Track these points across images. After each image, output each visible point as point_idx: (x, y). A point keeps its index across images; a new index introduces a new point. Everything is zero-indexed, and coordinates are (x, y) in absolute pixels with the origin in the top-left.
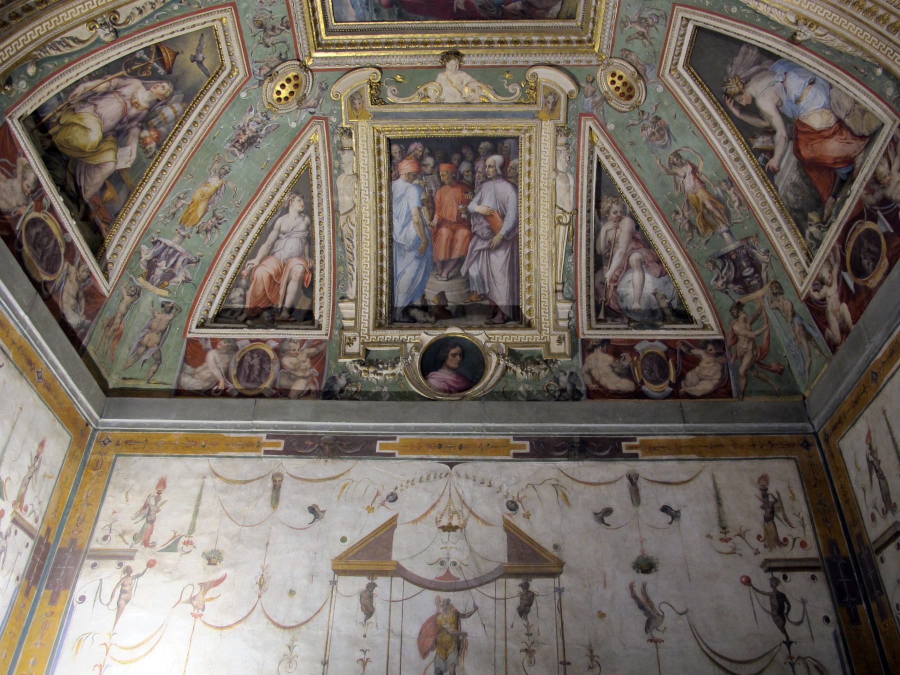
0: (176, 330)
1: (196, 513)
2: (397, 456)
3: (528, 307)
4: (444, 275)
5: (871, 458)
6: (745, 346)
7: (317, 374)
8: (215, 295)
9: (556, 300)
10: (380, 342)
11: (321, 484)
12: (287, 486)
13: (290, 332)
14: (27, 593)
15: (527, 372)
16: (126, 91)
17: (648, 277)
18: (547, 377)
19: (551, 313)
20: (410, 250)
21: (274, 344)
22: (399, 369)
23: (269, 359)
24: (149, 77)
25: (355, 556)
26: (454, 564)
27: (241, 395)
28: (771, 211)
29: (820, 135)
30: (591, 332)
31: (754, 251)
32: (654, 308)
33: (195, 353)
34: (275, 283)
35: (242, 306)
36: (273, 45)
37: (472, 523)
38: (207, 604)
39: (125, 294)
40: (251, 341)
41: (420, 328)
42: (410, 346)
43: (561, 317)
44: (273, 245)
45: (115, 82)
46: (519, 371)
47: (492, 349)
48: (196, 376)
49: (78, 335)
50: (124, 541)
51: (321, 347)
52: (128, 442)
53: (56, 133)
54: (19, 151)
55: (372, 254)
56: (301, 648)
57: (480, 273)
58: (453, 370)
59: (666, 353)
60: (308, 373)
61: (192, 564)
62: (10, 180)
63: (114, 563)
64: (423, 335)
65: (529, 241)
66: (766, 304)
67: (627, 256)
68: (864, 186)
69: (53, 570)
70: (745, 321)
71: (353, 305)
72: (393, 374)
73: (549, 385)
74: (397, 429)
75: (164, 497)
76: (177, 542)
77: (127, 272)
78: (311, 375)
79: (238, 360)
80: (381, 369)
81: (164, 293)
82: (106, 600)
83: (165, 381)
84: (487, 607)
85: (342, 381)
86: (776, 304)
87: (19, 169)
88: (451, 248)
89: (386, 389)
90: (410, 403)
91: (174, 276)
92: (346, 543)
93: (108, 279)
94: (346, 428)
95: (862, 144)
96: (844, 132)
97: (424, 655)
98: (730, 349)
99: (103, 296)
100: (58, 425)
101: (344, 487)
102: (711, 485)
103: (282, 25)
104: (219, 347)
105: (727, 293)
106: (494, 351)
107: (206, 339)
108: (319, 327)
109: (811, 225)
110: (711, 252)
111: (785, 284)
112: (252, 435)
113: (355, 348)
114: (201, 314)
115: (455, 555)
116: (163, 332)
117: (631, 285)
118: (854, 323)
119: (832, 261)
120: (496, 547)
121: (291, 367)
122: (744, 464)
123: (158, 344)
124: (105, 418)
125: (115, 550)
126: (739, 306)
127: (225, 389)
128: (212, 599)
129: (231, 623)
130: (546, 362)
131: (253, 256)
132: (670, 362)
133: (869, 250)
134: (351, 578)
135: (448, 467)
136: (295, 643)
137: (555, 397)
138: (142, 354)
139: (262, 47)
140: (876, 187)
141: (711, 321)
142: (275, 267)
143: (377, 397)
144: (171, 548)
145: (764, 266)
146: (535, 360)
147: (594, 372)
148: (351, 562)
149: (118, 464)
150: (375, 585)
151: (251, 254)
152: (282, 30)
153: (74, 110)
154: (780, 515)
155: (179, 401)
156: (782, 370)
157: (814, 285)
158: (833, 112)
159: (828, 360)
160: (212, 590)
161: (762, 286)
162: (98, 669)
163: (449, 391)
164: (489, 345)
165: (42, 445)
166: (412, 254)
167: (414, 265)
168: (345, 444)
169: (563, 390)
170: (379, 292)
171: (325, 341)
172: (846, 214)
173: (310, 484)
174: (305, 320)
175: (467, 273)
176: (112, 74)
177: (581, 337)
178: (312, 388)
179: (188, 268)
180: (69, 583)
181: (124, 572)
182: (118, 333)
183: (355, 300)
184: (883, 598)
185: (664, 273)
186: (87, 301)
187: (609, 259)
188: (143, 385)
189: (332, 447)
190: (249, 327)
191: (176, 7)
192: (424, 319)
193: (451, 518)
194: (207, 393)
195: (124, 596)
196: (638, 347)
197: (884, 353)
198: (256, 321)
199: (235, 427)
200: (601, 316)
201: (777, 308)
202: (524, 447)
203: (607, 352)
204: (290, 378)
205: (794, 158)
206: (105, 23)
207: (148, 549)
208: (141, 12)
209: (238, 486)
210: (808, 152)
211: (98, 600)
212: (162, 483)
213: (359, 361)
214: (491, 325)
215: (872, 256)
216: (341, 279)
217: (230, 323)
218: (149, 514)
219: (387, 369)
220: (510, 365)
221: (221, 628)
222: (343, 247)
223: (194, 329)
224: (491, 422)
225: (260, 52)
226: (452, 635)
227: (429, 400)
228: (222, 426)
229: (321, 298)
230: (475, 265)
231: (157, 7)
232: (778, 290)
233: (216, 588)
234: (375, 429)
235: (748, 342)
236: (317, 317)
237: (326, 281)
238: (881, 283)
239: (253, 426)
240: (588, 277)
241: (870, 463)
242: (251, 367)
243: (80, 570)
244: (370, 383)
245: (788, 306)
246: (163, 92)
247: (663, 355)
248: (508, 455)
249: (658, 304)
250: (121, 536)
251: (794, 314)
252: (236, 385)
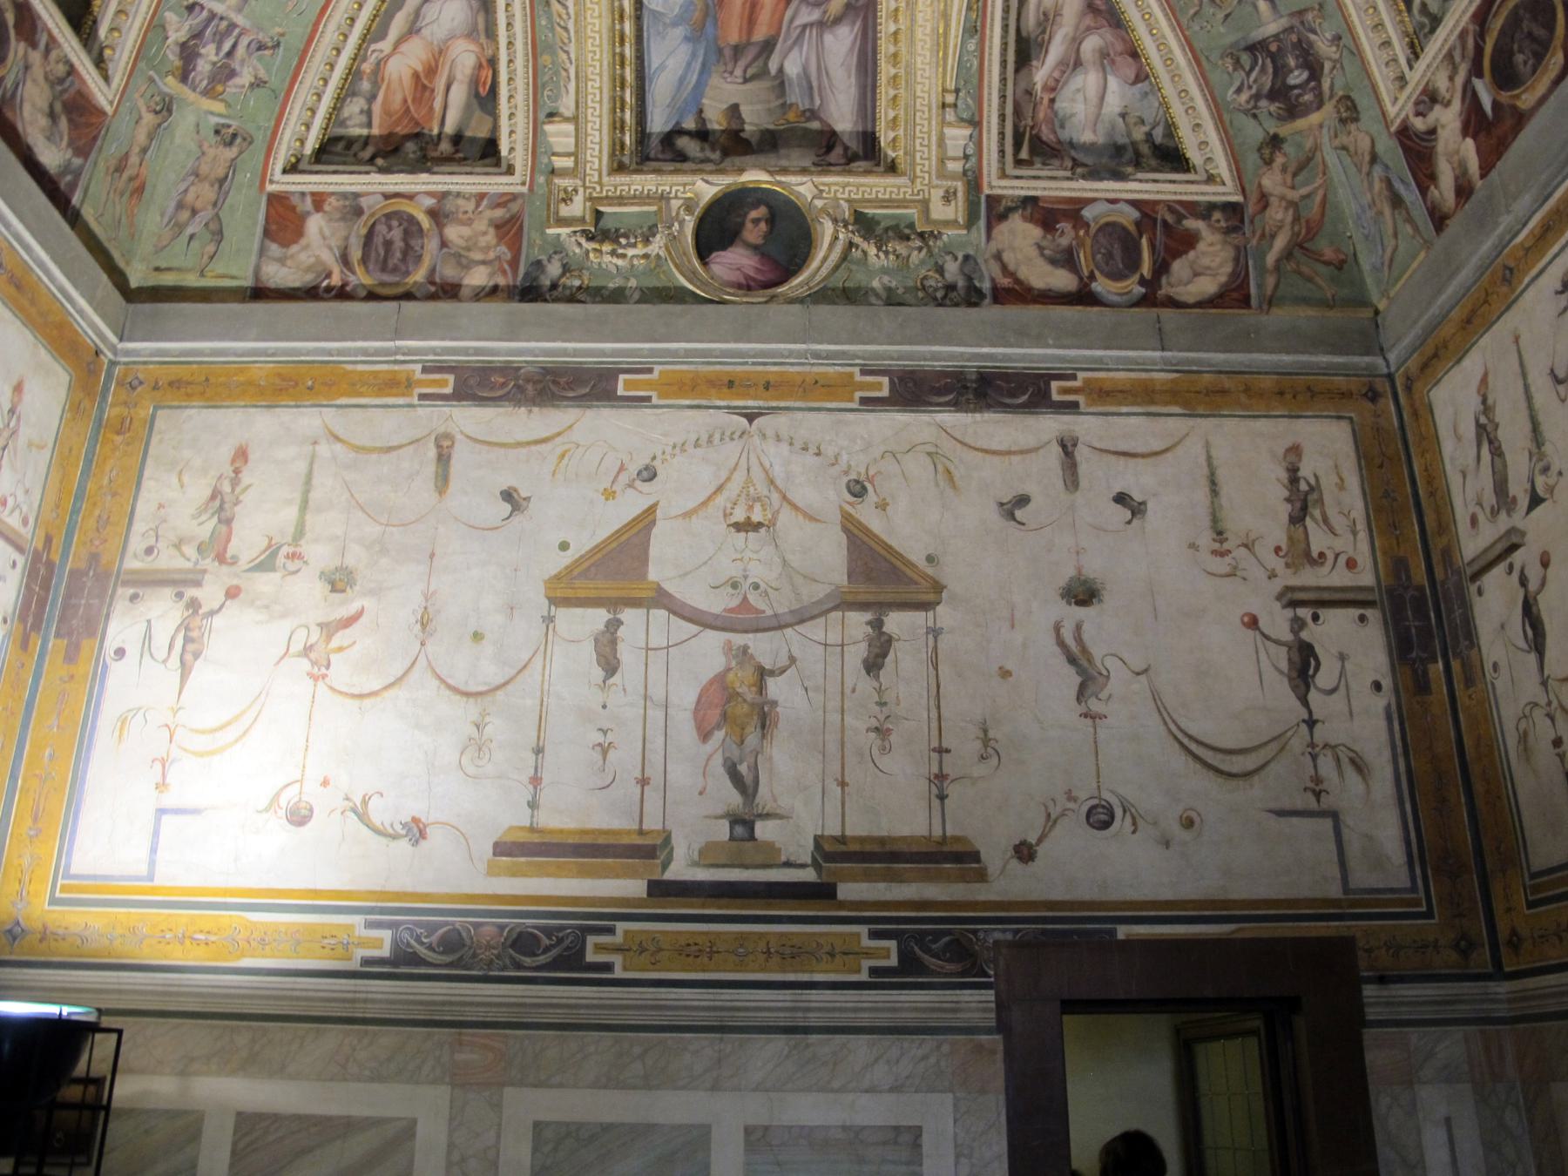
0: (245, 177)
1: (304, 505)
2: (655, 401)
3: (891, 135)
4: (738, 72)
5: (1483, 420)
6: (1279, 216)
7: (509, 256)
8: (313, 111)
9: (944, 123)
10: (621, 197)
11: (524, 451)
12: (462, 456)
13: (455, 179)
14: (25, 644)
15: (887, 253)
17: (1113, 83)
18: (923, 262)
19: (935, 148)
20: (675, 24)
21: (429, 202)
22: (657, 246)
23: (421, 230)
25: (584, 574)
26: (756, 587)
27: (372, 296)
30: (1004, 183)
31: (1312, 37)
32: (1122, 140)
33: (283, 221)
34: (425, 87)
35: (365, 132)
37: (786, 517)
38: (333, 657)
39: (143, 109)
40: (387, 196)
41: (694, 172)
42: (675, 204)
43: (950, 153)
44: (417, 14)
46: (872, 251)
47: (824, 210)
48: (289, 262)
49: (62, 186)
50: (183, 555)
51: (515, 207)
52: (176, 384)
55: (604, 31)
56: (496, 728)
57: (805, 69)
58: (755, 248)
59: (1138, 224)
60: (492, 255)
61: (306, 591)
63: (168, 592)
64: (700, 185)
65: (897, 10)
66: (1325, 139)
67: (1076, 42)
69: (65, 607)
70: (1284, 169)
71: (570, 127)
72: (646, 256)
73: (925, 278)
74: (653, 353)
75: (246, 478)
76: (274, 555)
77: (142, 65)
78: (498, 258)
79: (364, 231)
80: (624, 247)
81: (218, 107)
82: (161, 653)
83: (234, 272)
84: (810, 658)
85: (554, 269)
86: (1344, 139)
88: (751, 21)
89: (633, 283)
90: (678, 308)
91: (232, 74)
92: (569, 552)
93: (107, 79)
94: (565, 353)
97: (705, 736)
98: (1252, 222)
99: (104, 113)
100: (44, 355)
101: (563, 456)
102: (1202, 459)
104: (327, 208)
105: (1255, 116)
106: (828, 214)
107: (303, 194)
108: (510, 170)
110: (1231, 39)
111: (1363, 101)
112: (396, 367)
113: (577, 207)
114: (289, 148)
115: (757, 572)
116: (222, 181)
117: (1080, 97)
118: (1482, 176)
119: (1457, 58)
120: (828, 559)
121: (462, 243)
122: (1261, 424)
123: (215, 204)
124: (130, 340)
125: (168, 571)
126: (1275, 142)
127: (343, 286)
128: (340, 649)
129: (376, 686)
130: (921, 235)
131: (382, 35)
132: (1144, 241)
134: (579, 611)
135: (744, 421)
136: (487, 719)
137: (935, 299)
138: (187, 224)
141: (1222, 168)
142: (424, 57)
143: (617, 296)
144: (266, 564)
145: (1327, 66)
146: (901, 232)
147: (1006, 257)
148: (578, 583)
149: (159, 424)
150: (619, 623)
151: (375, 33)
154: (1317, 513)
155: (260, 308)
156: (1343, 262)
157: (1417, 103)
159: (1428, 245)
160: (340, 634)
161: (1320, 106)
162: (158, 766)
163: (747, 286)
164: (819, 203)
165: (18, 388)
166: (679, 32)
167: (684, 51)
168: (562, 380)
169: (951, 288)
170: (617, 104)
171: (522, 195)
173: (502, 451)
174: (483, 156)
175: (781, 70)
177: (987, 191)
178: (501, 281)
179: (260, 59)
180: (94, 626)
181: (188, 607)
182: (136, 184)
183: (575, 120)
184: (1474, 652)
185: (1141, 77)
186: (70, 121)
187: (1043, 46)
188: (192, 280)
189: (539, 386)
190: (382, 171)
192: (699, 155)
193: (751, 508)
194: (311, 293)
195: (191, 647)
196: (1087, 213)
197: (1532, 231)
198: (392, 160)
199: (365, 352)
200: (1024, 155)
201: (1344, 148)
202: (879, 386)
203: (1031, 219)
204: (459, 264)
207: (225, 568)
209: (374, 456)
211: (146, 654)
212: (241, 455)
213: (583, 231)
214: (823, 167)
216: (546, 78)
217: (344, 163)
218: (221, 508)
219: (634, 245)
220: (857, 240)
221: (361, 696)
222: (550, 18)
223: (278, 175)
224: (821, 343)
226: (753, 705)
227: (711, 302)
228: (340, 352)
229: (511, 116)
230: (795, 54)
232: (1350, 112)
233: (347, 631)
234: (615, 353)
235: (1286, 209)
236: (504, 152)
237: (520, 83)
238: (1543, 100)
239: (397, 351)
240: (1003, 80)
241: (1480, 428)
242: (388, 244)
243: (110, 605)
244: (606, 273)
245: (1365, 144)
247: (1132, 228)
248: (851, 400)
249: (1129, 134)
250: (177, 546)
251: (1374, 158)
252: (362, 278)
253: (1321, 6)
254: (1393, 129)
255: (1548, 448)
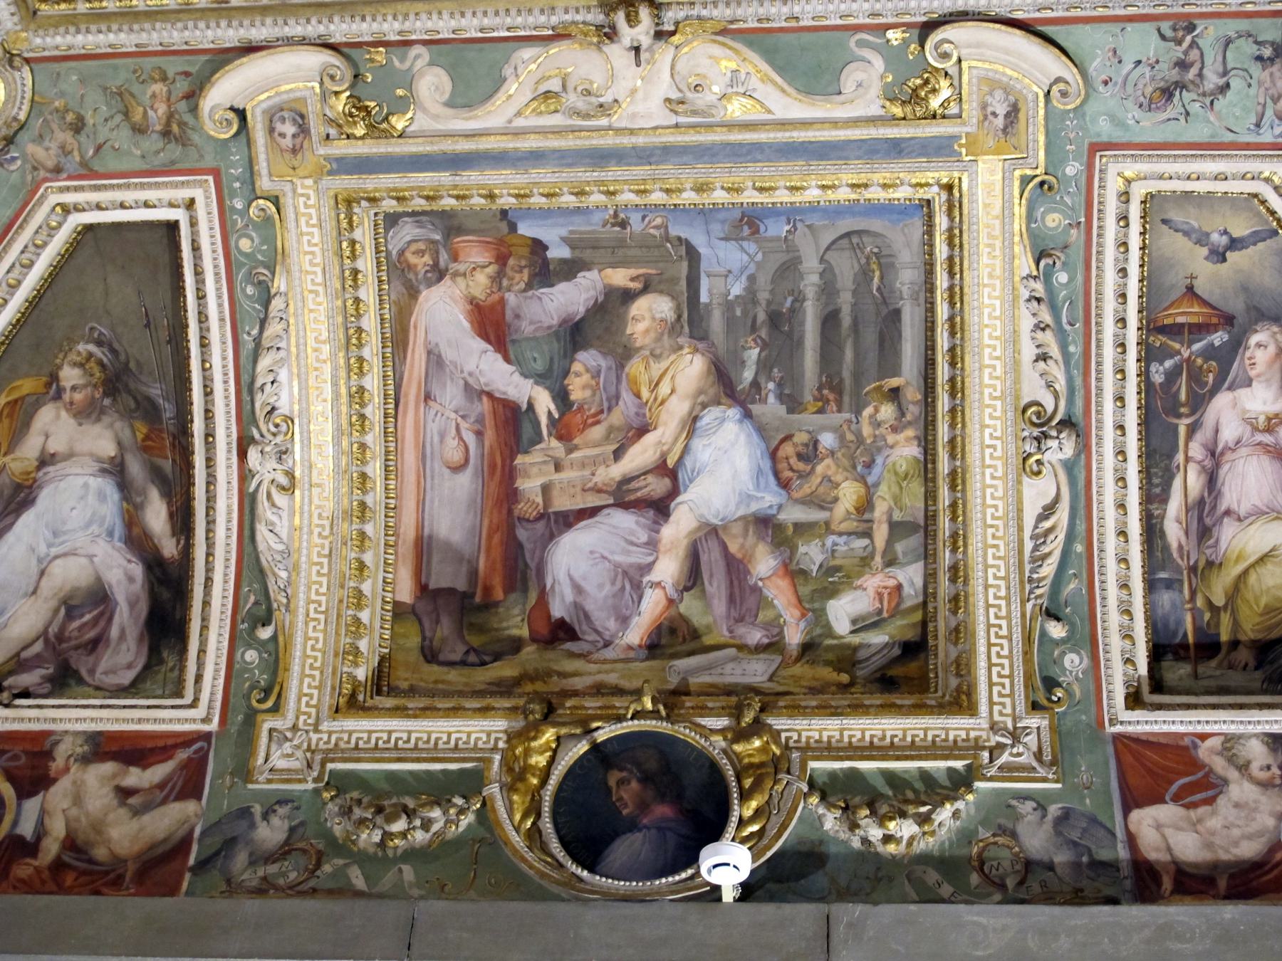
16: (1229, 434)
24: (1224, 368)
36: (1225, 73)
45: (1196, 450)
53: (1236, 624)
54: (1187, 741)
62: (1221, 801)
87: (1219, 765)
103: (1179, 43)
139: (1221, 103)
152: (1194, 44)
153: (1210, 564)
176: (1174, 449)
191: (1063, 277)
206: (1037, 439)
208: (1044, 357)
225: (1236, 111)
231: (1047, 318)
246: (1272, 349)
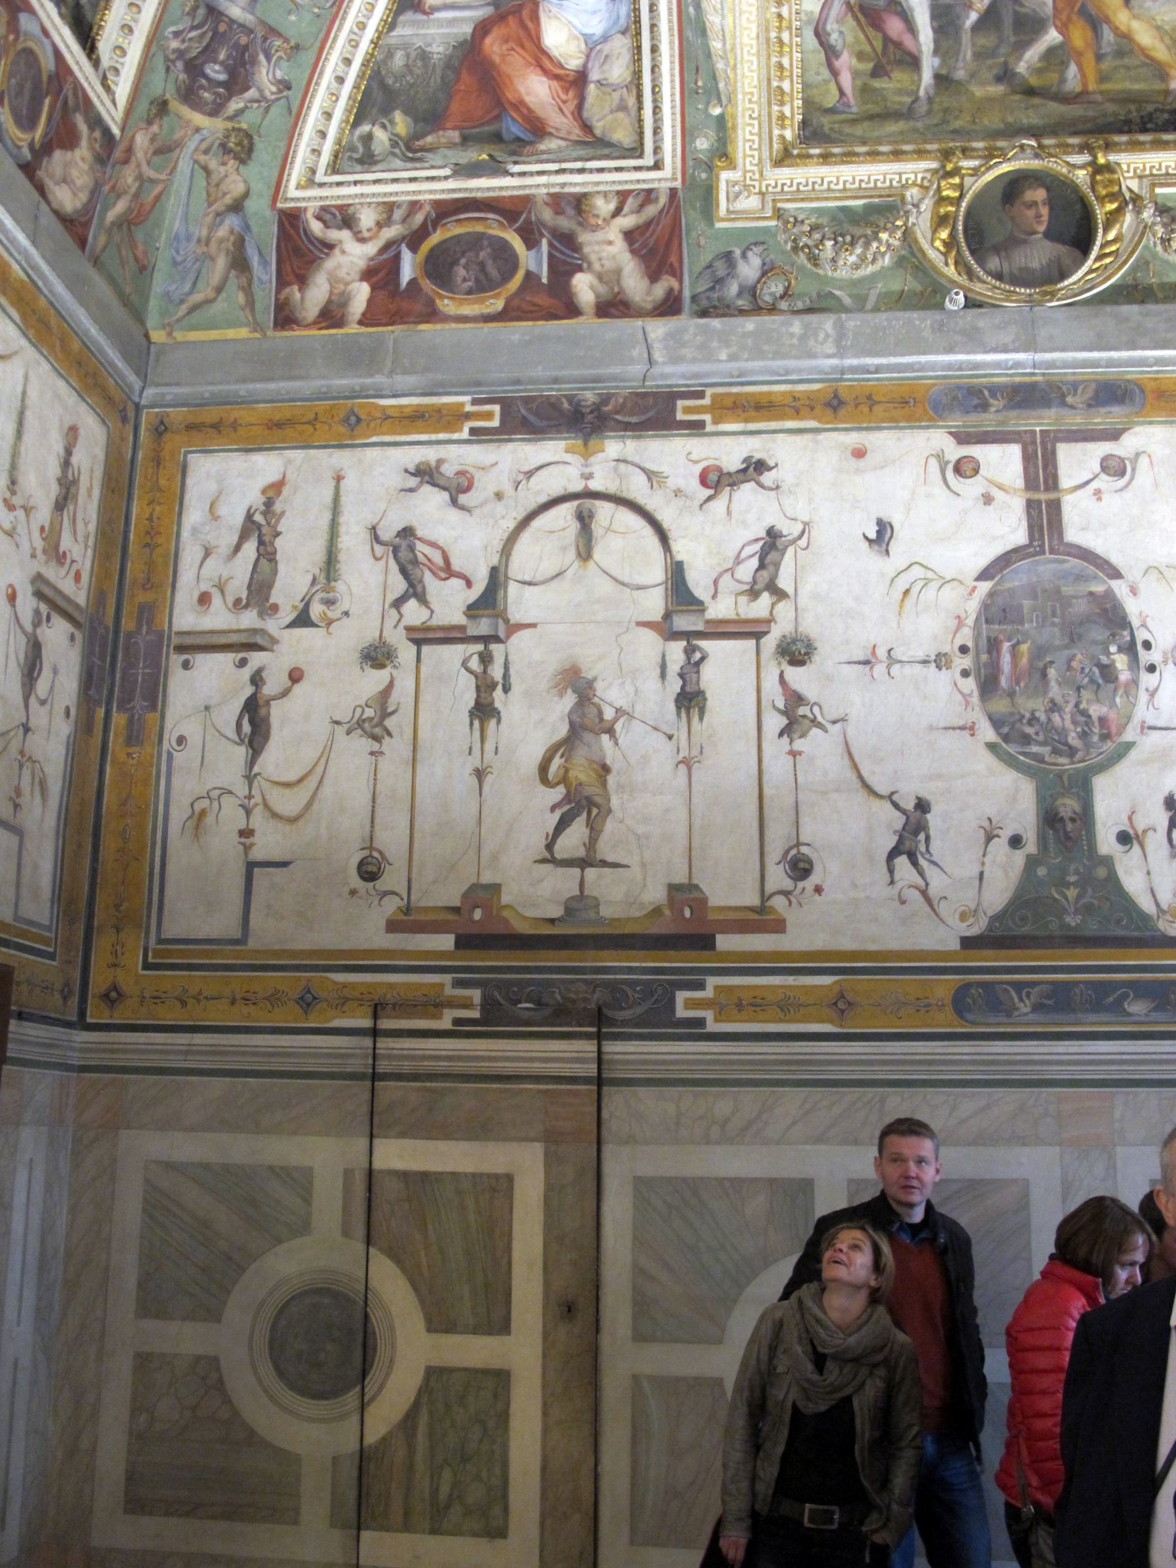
5: (258, 518)
28: (356, 47)
29: (542, 60)
31: (262, 58)
66: (192, 145)
68: (552, 190)
86: (213, 164)
95: (577, 133)
96: (571, 94)
102: (19, 389)
105: (168, 69)
109: (384, 127)
111: (264, 153)
118: (360, 323)
119: (398, 214)
122: (61, 385)
126: (162, 107)
132: (47, 101)
133: (482, 266)
140: (570, 211)
141: (123, 89)
145: (252, 93)
154: (71, 507)
158: (588, 56)
159: (256, 326)
161: (214, 112)
172: (489, 189)
184: (152, 718)
197: (401, 407)
201: (205, 169)
205: (468, 29)
210: (496, 48)
215: (482, 277)
232: (241, 148)
241: (250, 526)
245: (238, 188)
251: (237, 207)
253: (297, 47)
254: (279, 205)
255: (340, 586)
